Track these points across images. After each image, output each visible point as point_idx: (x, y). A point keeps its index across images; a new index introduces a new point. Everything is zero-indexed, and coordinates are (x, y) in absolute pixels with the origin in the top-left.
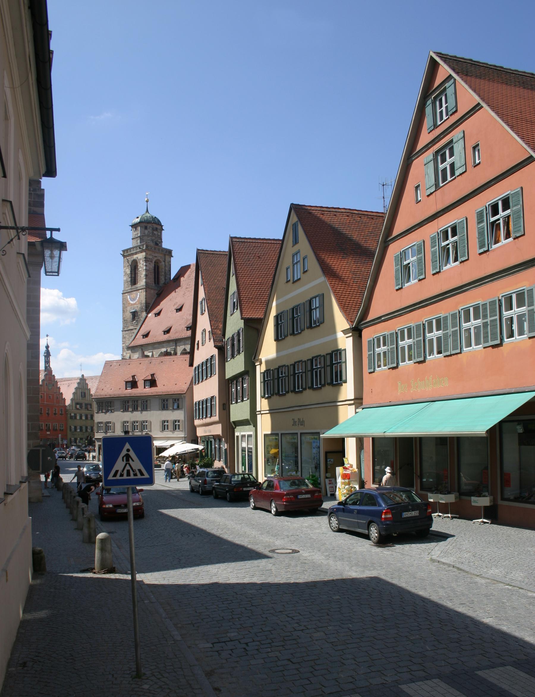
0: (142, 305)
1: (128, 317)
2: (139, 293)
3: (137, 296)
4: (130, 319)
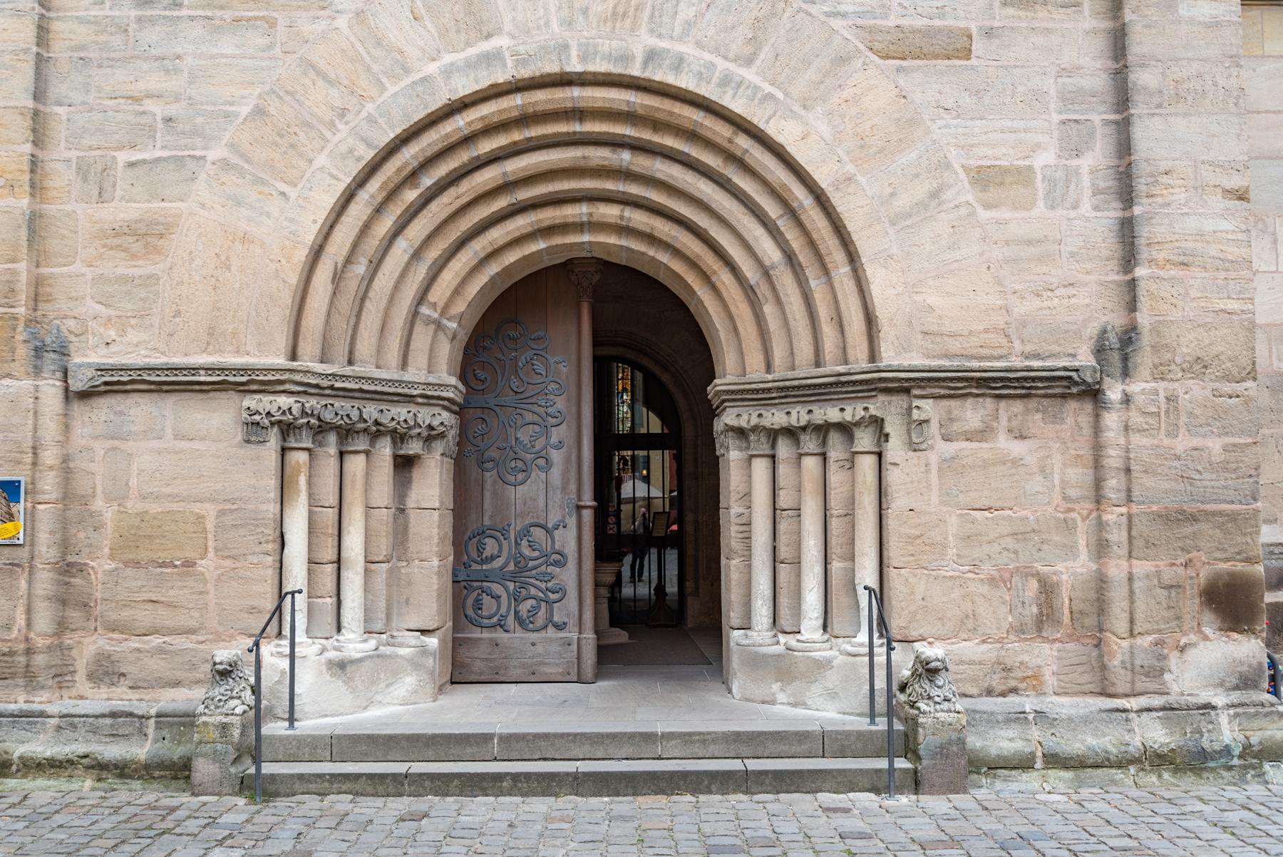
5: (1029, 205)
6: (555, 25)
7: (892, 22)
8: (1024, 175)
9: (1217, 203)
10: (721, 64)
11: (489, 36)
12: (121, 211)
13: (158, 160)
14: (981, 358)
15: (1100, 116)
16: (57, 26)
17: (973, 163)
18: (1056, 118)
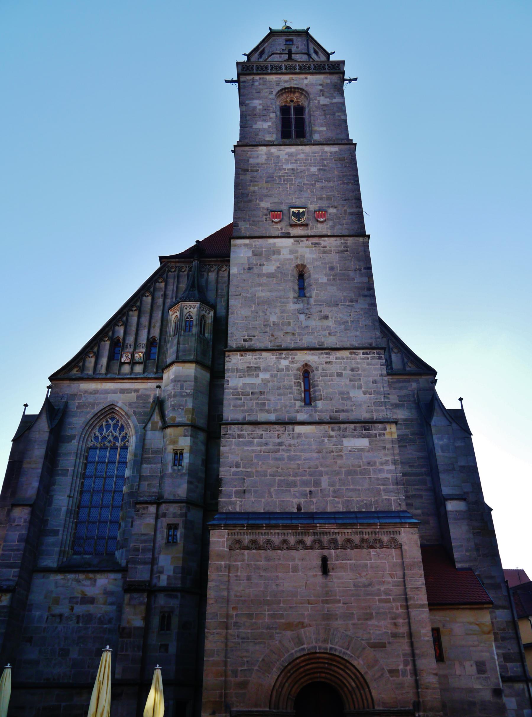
5: (399, 677)
6: (314, 643)
7: (372, 641)
8: (397, 671)
9: (432, 676)
10: (343, 650)
11: (302, 645)
12: (240, 679)
13: (246, 669)
14: (393, 708)
15: (410, 659)
16: (229, 643)
17: (388, 668)
18: (402, 659)
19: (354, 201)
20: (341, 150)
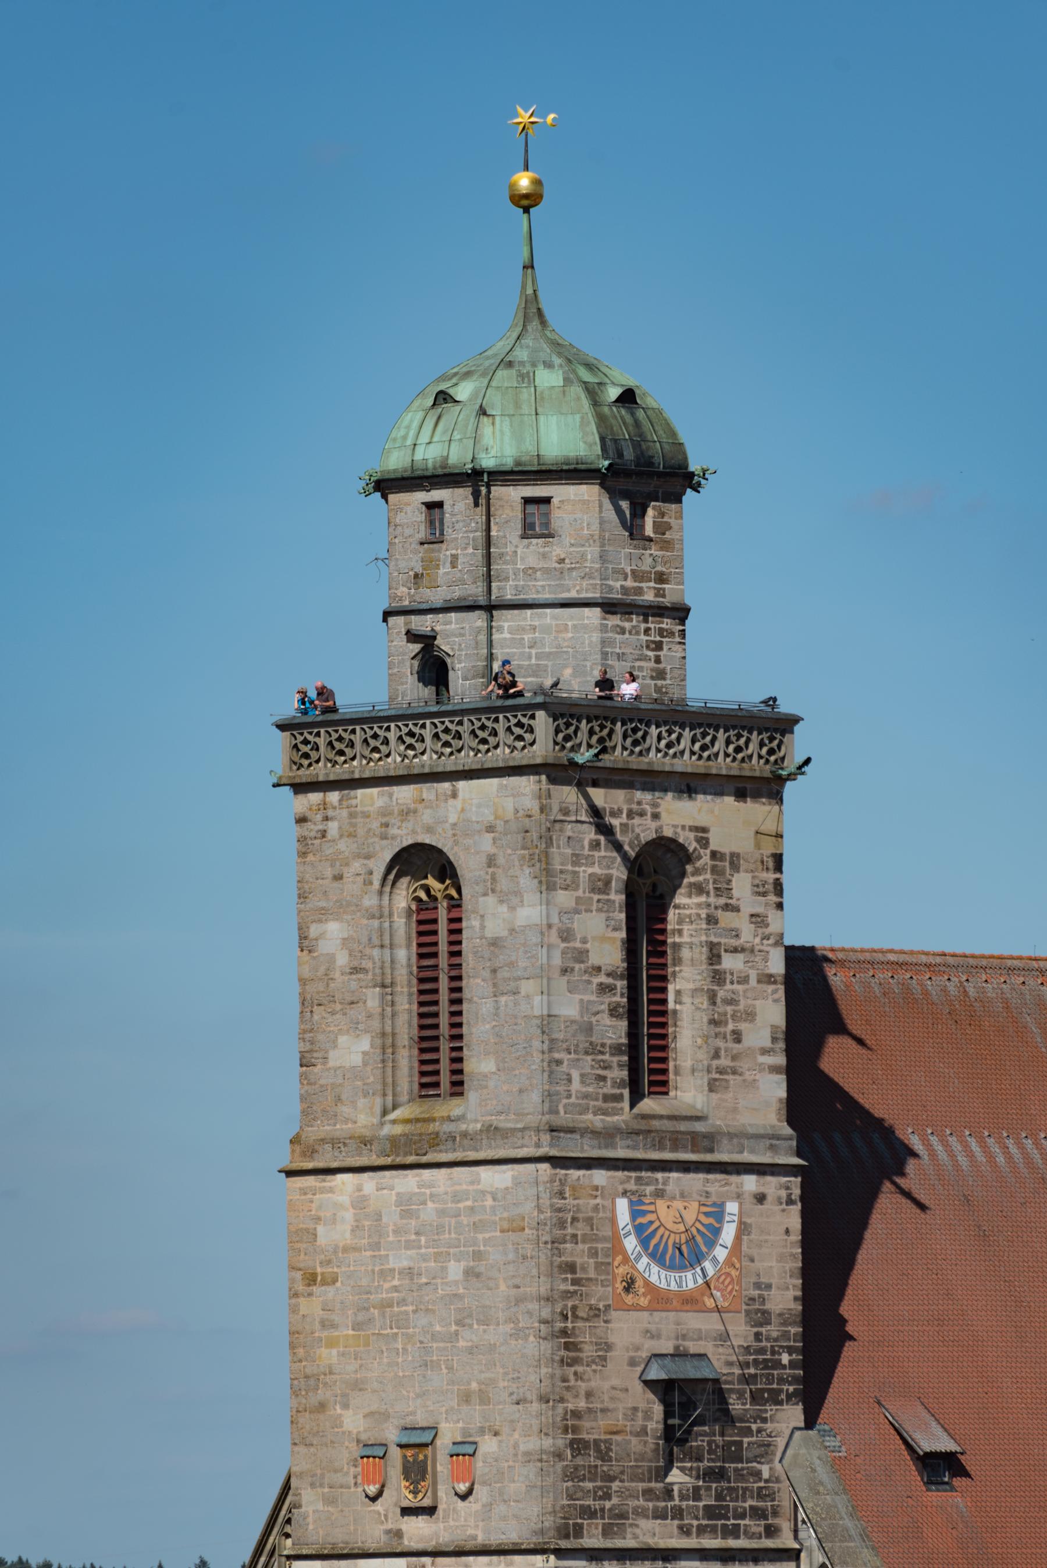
0: (773, 1330)
1: (618, 1419)
2: (739, 1196)
3: (717, 1232)
4: (635, 1444)
19: (535, 1407)
20: (517, 1183)
